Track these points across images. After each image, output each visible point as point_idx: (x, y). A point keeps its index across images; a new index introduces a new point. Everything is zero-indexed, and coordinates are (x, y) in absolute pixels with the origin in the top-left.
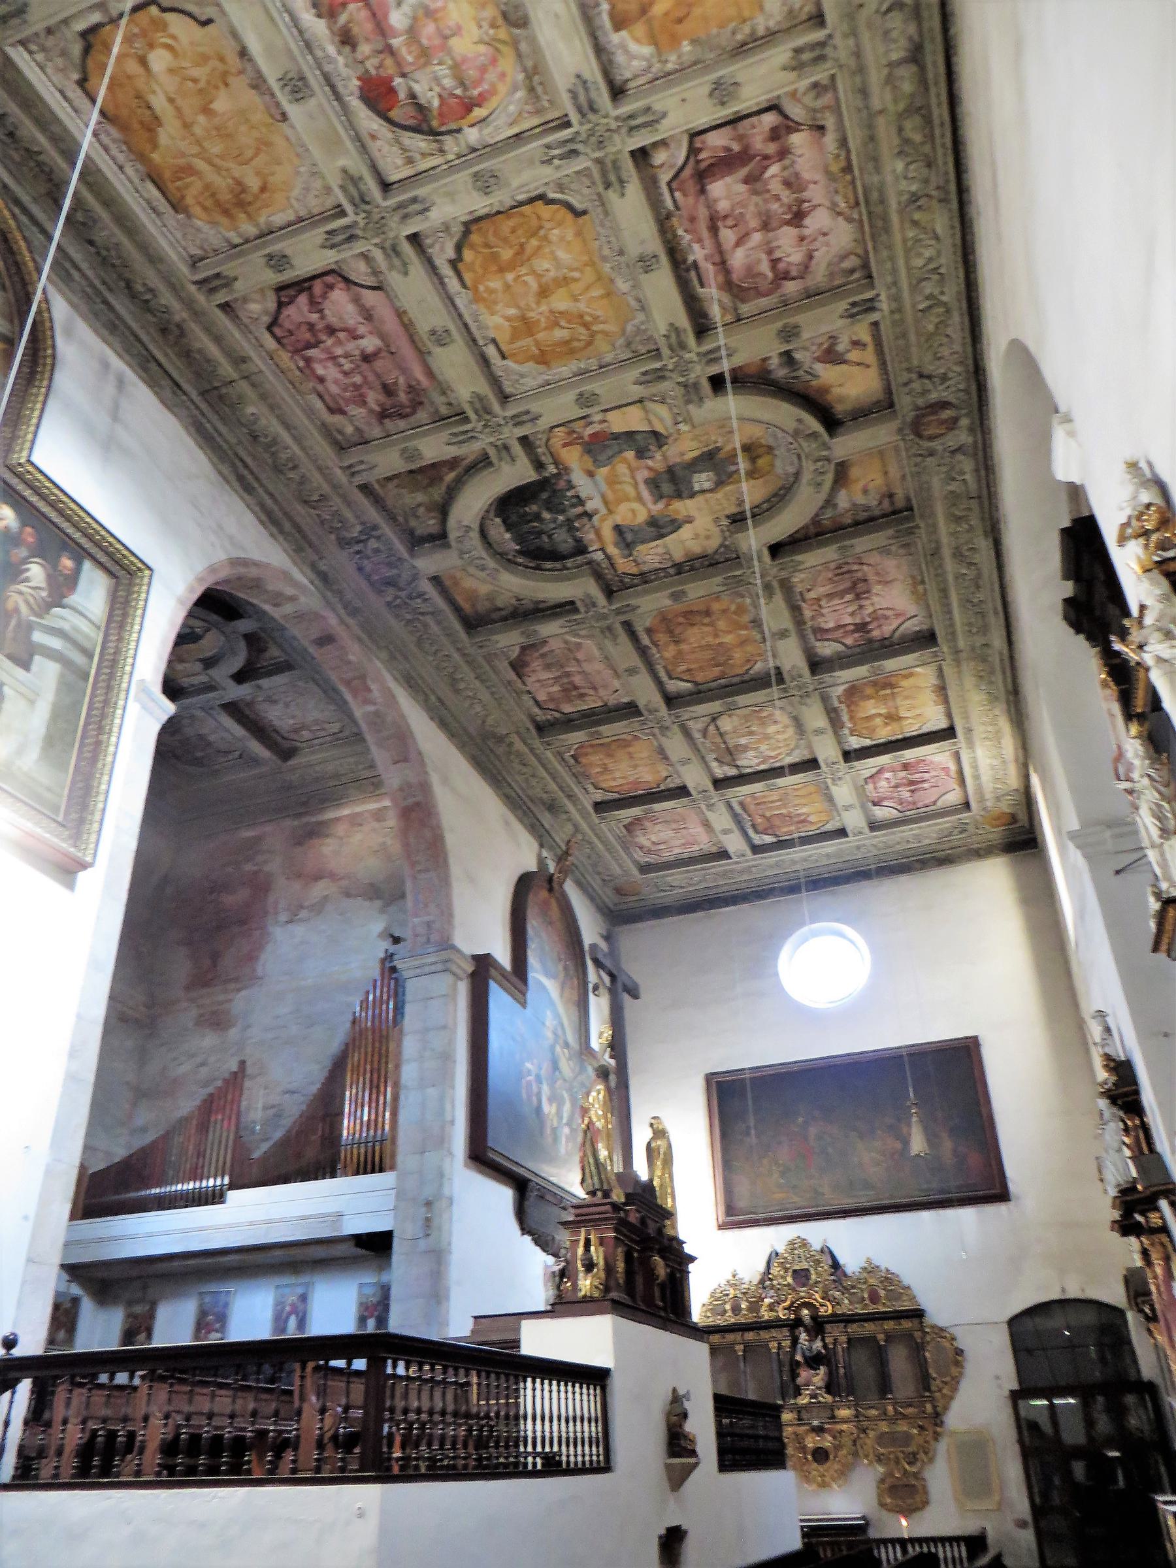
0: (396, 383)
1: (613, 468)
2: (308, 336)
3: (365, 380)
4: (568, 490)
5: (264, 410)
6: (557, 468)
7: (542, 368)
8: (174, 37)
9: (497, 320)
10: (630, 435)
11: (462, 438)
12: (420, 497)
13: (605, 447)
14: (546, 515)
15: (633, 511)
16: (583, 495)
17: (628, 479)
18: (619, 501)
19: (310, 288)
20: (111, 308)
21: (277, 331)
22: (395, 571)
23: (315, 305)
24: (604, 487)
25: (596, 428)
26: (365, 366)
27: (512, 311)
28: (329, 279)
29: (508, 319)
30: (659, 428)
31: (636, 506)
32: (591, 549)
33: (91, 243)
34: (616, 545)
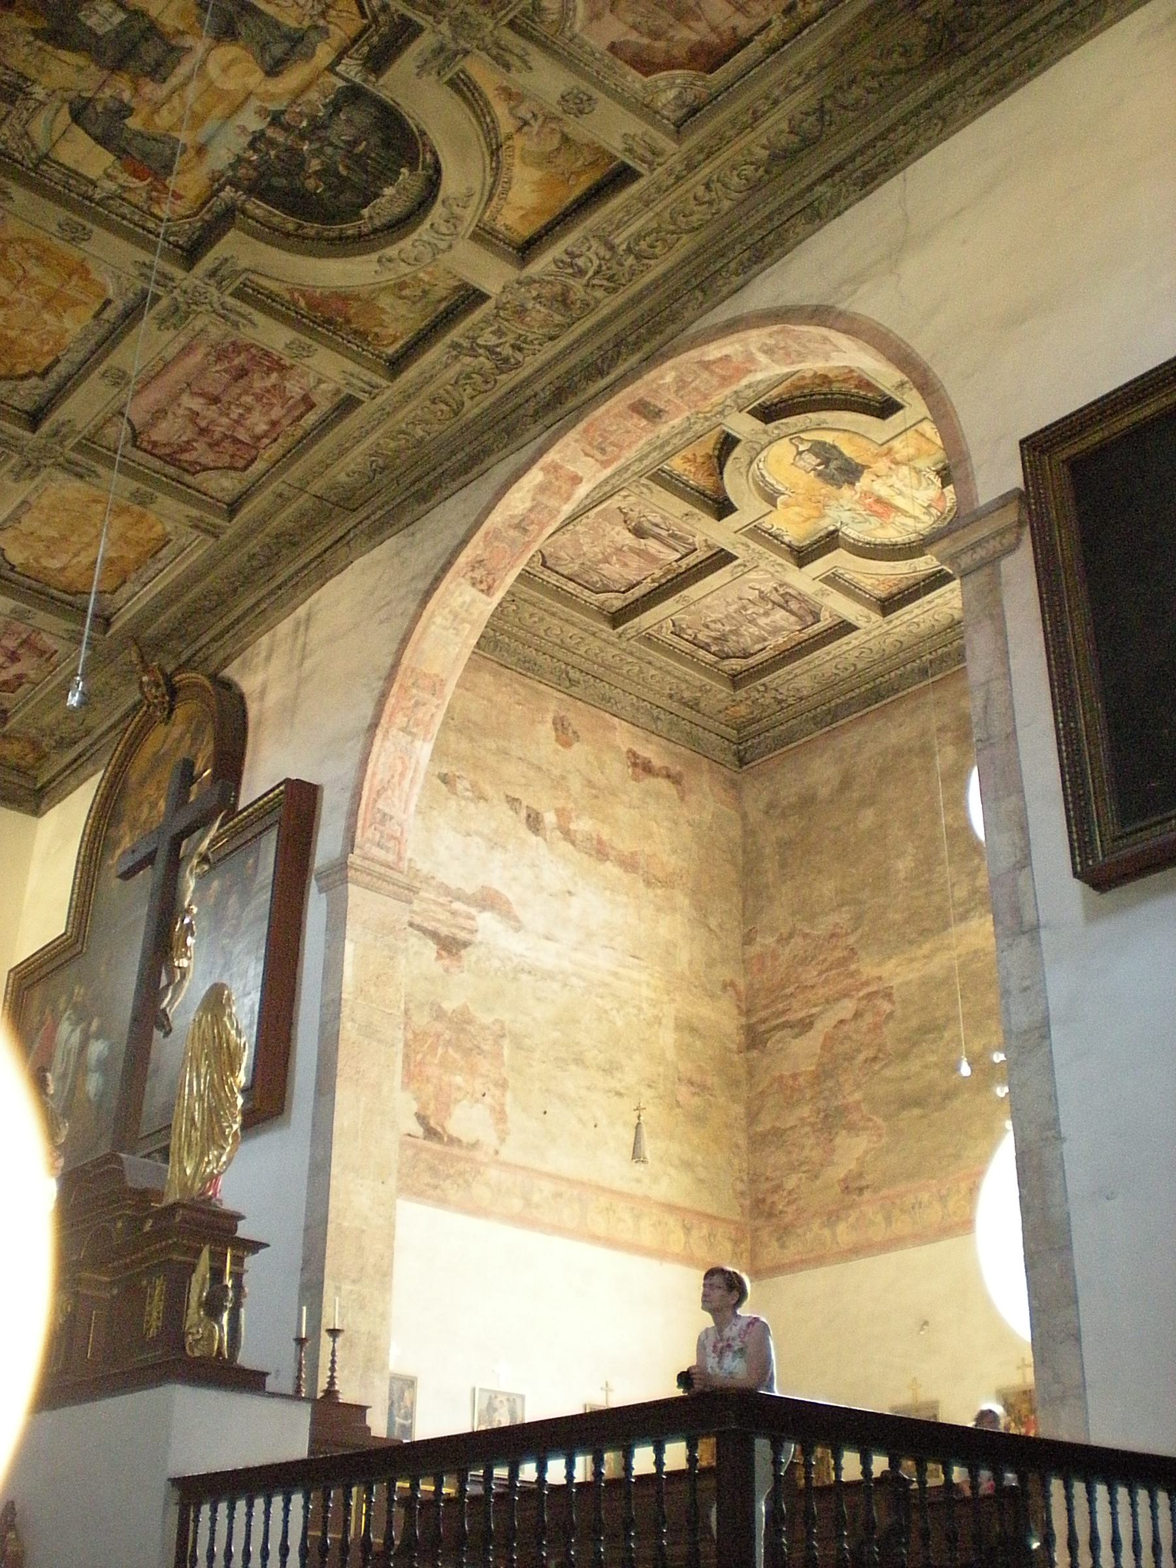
0: (225, 371)
1: (171, 128)
2: (226, 444)
3: (246, 392)
4: (250, 162)
5: (333, 471)
6: (221, 188)
7: (90, 265)
8: (27, 559)
9: (68, 323)
10: (103, 141)
11: (233, 317)
12: (385, 301)
13: (146, 155)
14: (315, 165)
15: (225, 70)
16: (245, 140)
17: (176, 100)
18: (222, 95)
19: (169, 455)
20: (285, 583)
21: (241, 463)
22: (530, 305)
23: (186, 447)
24: (210, 125)
25: (124, 178)
26: (225, 399)
27: (46, 316)
28: (145, 445)
29: (59, 317)
30: (65, 117)
31: (213, 70)
32: (341, 83)
33: (235, 590)
34: (309, 56)
